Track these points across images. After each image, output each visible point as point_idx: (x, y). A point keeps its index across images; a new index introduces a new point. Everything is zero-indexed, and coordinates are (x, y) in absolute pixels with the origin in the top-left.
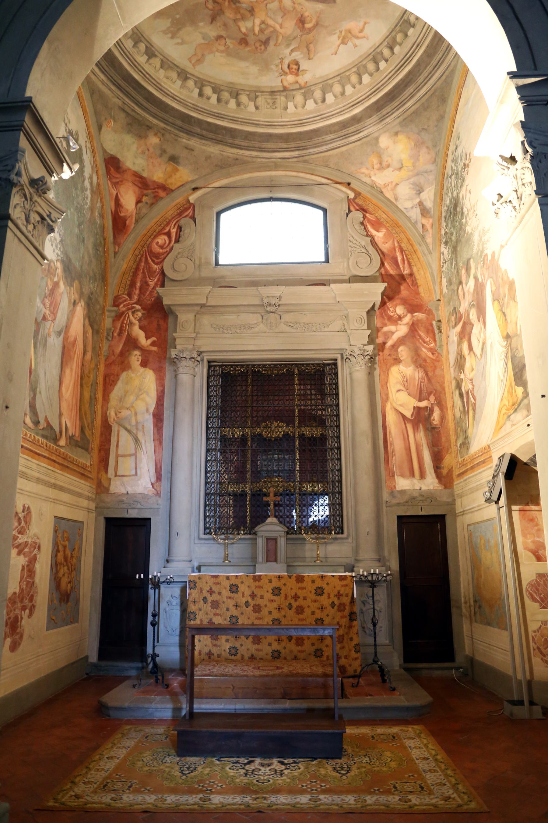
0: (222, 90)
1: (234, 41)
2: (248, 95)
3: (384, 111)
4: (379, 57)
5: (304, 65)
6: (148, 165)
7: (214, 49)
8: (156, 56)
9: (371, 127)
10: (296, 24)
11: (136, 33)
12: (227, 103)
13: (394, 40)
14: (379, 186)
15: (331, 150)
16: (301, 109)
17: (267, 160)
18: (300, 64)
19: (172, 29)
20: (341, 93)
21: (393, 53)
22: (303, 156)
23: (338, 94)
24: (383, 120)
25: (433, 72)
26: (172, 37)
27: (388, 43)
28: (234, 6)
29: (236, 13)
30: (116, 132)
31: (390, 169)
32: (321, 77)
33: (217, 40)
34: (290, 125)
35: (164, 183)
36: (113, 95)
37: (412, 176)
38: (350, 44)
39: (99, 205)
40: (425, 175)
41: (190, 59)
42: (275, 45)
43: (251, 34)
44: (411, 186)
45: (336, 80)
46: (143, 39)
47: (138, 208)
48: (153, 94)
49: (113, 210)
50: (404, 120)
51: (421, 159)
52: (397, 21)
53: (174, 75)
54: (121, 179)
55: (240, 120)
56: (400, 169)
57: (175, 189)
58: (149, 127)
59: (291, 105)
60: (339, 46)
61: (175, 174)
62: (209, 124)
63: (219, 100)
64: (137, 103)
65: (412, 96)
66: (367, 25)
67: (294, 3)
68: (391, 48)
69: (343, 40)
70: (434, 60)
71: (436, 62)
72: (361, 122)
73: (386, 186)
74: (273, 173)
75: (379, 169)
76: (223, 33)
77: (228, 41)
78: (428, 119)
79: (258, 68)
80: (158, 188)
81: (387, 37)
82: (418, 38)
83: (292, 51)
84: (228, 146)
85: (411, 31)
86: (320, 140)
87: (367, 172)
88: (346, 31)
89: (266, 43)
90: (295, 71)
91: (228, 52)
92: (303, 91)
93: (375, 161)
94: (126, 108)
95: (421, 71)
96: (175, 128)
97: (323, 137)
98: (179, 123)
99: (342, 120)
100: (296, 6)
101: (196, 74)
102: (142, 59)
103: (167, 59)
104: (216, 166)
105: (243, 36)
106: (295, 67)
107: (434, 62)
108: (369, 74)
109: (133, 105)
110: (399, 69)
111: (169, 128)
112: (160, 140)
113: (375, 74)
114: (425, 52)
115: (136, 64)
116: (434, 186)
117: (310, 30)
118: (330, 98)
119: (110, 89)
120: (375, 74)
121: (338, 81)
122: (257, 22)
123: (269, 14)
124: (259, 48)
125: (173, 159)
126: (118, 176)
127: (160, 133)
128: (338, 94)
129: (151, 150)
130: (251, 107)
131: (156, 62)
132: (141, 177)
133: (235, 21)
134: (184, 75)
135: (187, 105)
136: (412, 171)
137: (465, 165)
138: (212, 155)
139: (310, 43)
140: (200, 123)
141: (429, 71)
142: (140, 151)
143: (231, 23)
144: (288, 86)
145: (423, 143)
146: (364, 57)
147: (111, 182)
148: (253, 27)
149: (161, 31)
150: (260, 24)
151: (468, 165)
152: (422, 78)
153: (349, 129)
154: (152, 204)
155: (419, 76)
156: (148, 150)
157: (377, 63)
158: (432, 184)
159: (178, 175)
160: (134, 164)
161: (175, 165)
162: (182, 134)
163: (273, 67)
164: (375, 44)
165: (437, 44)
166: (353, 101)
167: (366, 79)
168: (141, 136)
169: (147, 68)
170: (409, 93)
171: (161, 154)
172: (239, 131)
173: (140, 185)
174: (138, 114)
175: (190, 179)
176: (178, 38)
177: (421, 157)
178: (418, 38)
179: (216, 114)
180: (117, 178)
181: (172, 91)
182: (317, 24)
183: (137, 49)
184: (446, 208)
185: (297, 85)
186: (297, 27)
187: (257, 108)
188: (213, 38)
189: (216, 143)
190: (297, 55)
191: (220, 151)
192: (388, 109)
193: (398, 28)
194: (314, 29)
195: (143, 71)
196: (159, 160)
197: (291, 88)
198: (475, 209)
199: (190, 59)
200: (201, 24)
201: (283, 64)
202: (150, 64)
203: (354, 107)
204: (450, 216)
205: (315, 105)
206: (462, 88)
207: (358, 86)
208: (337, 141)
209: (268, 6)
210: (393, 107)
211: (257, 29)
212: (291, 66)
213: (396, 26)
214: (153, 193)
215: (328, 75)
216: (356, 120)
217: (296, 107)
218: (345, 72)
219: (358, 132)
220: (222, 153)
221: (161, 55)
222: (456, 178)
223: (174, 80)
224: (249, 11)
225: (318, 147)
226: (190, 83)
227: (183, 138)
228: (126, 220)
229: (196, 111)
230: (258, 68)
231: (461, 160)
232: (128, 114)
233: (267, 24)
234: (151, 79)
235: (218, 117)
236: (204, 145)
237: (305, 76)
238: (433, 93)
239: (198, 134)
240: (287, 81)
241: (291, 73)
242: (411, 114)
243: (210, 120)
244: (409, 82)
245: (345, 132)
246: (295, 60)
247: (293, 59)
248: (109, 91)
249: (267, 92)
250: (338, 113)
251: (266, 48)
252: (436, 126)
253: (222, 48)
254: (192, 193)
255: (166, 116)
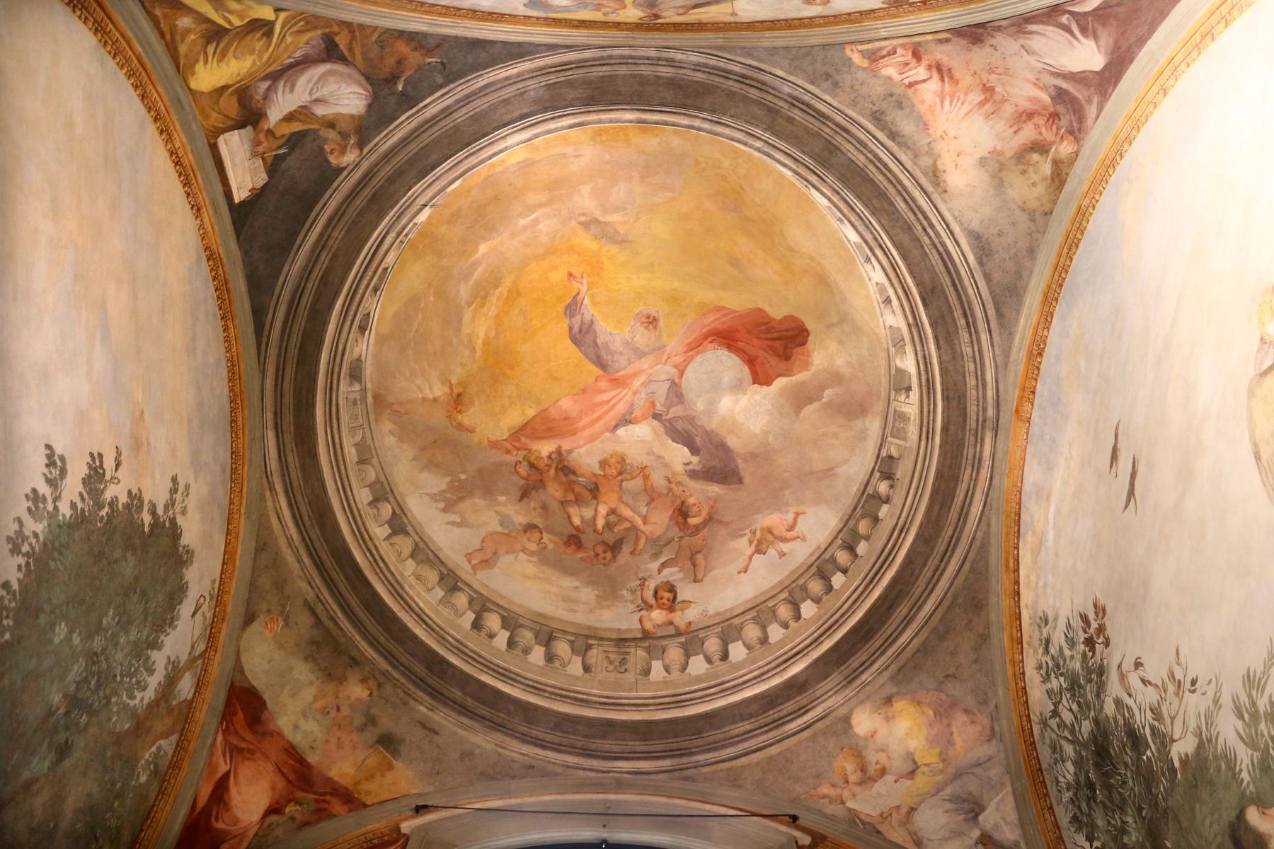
0: (522, 626)
1: (557, 539)
2: (572, 642)
3: (854, 662)
4: (830, 567)
5: (685, 592)
6: (327, 741)
7: (519, 547)
8: (407, 533)
9: (830, 696)
10: (671, 518)
11: (382, 483)
12: (527, 651)
13: (854, 532)
14: (868, 820)
15: (745, 754)
16: (679, 673)
17: (601, 775)
18: (678, 591)
19: (448, 495)
20: (759, 639)
21: (856, 556)
22: (681, 769)
23: (754, 642)
24: (855, 678)
25: (943, 564)
26: (445, 510)
27: (844, 541)
28: (564, 479)
29: (566, 491)
30: (281, 647)
31: (889, 778)
32: (719, 614)
33: (525, 532)
34: (655, 705)
35: (351, 788)
36: (301, 574)
37: (946, 784)
38: (772, 552)
39: (167, 745)
40: (978, 771)
41: (469, 556)
42: (631, 553)
43: (589, 530)
44: (948, 805)
45: (748, 617)
46: (391, 499)
47: (266, 824)
48: (382, 600)
49: (202, 802)
50: (899, 670)
51: (958, 741)
52: (855, 501)
53: (433, 577)
54: (252, 747)
55: (548, 689)
56: (912, 774)
57: (374, 804)
58: (355, 662)
59: (657, 667)
60: (751, 558)
61: (383, 776)
62: (484, 686)
63: (511, 643)
64: (346, 607)
65: (908, 621)
66: (800, 519)
67: (670, 482)
68: (851, 549)
69: (757, 546)
70: (939, 545)
71: (943, 548)
72: (805, 691)
73: (884, 817)
74: (612, 797)
75: (860, 784)
76: (538, 521)
77: (546, 537)
78: (954, 653)
79: (596, 592)
80: (332, 794)
81: (840, 531)
82: (899, 518)
83: (663, 565)
84: (516, 738)
85: (884, 511)
86: (717, 735)
87: (832, 792)
88: (762, 529)
89: (615, 548)
90: (669, 603)
91: (544, 558)
92: (682, 639)
93: (850, 767)
94: (320, 609)
95: (917, 572)
96: (409, 678)
97: (727, 729)
98: (420, 669)
99: (765, 691)
100: (673, 486)
101: (476, 585)
102: (379, 532)
103: (426, 545)
104: (482, 774)
105: (574, 532)
106: (667, 595)
107: (940, 546)
108: (812, 600)
109: (335, 607)
110: (871, 581)
111: (396, 675)
112: (370, 695)
113: (825, 598)
114: (918, 536)
115: (366, 536)
116: (1009, 788)
117: (698, 529)
118: (737, 651)
119: (300, 561)
120: (825, 598)
121: (753, 618)
122: (603, 510)
123: (624, 498)
124: (602, 555)
125: (388, 743)
126: (248, 735)
127: (376, 680)
128: (754, 642)
129: (345, 710)
130: (576, 667)
131: (406, 545)
132: (301, 761)
133: (563, 503)
134: (451, 582)
135: (444, 639)
136: (942, 772)
137: (1090, 642)
138: (477, 751)
139: (697, 552)
140: (464, 680)
141: (933, 567)
142: (319, 704)
143: (555, 506)
144: (653, 630)
145: (954, 704)
146: (801, 571)
147: (225, 739)
148: (594, 518)
149: (427, 494)
150: (608, 515)
151: (1101, 629)
152: (921, 583)
153: (783, 707)
154: (306, 824)
155: (915, 583)
156: (338, 709)
157: (825, 578)
158: (1002, 785)
159: (390, 776)
160: (296, 727)
161: (389, 756)
162: (420, 694)
163: (624, 592)
164: (819, 547)
165: (939, 515)
166: (787, 653)
167: (808, 609)
168: (332, 676)
169: (384, 548)
170: (900, 619)
171: (365, 725)
172: (546, 710)
173: (292, 777)
174: (341, 628)
175: (414, 791)
176: (455, 513)
177: (955, 735)
178: (899, 518)
179: (500, 670)
180: (244, 740)
181: (421, 605)
182: (710, 520)
183: (375, 511)
184: (1067, 795)
185: (671, 627)
186: (673, 522)
187: (587, 669)
188: (519, 527)
189: (489, 727)
190: (671, 574)
191: (497, 745)
192: (862, 656)
193: (859, 512)
194: (704, 527)
195: (374, 552)
196: (355, 736)
197: (659, 634)
198: (1179, 675)
199: (469, 556)
200: (502, 499)
201: (645, 588)
202: (392, 544)
203: (788, 663)
204: (1092, 798)
205: (708, 666)
206: (1017, 548)
207: (792, 624)
208: (757, 735)
209: (624, 484)
210: (872, 650)
211: (600, 523)
212: (661, 593)
213: (855, 509)
214: (317, 801)
215: (732, 608)
216: (796, 687)
217: (667, 669)
218: (765, 601)
219: (802, 711)
220: (499, 750)
221: (417, 533)
222: (1073, 695)
223: (430, 586)
224: (590, 491)
225: (716, 749)
226: (461, 600)
227: (422, 704)
228: (223, 842)
229: (460, 654)
230: (596, 592)
231: (1072, 643)
232: (318, 622)
233: (620, 516)
234: (386, 571)
235: (504, 676)
236: (464, 727)
237: (686, 612)
238: (952, 603)
239: (455, 703)
240: (651, 620)
241: (660, 607)
242: (913, 656)
243: (485, 678)
244: (896, 598)
245: (773, 714)
246: (668, 582)
247: (665, 580)
248: (296, 566)
249: (610, 640)
250: (755, 678)
251: (614, 557)
252: (976, 661)
253: (533, 547)
254: (412, 817)
255: (399, 651)
